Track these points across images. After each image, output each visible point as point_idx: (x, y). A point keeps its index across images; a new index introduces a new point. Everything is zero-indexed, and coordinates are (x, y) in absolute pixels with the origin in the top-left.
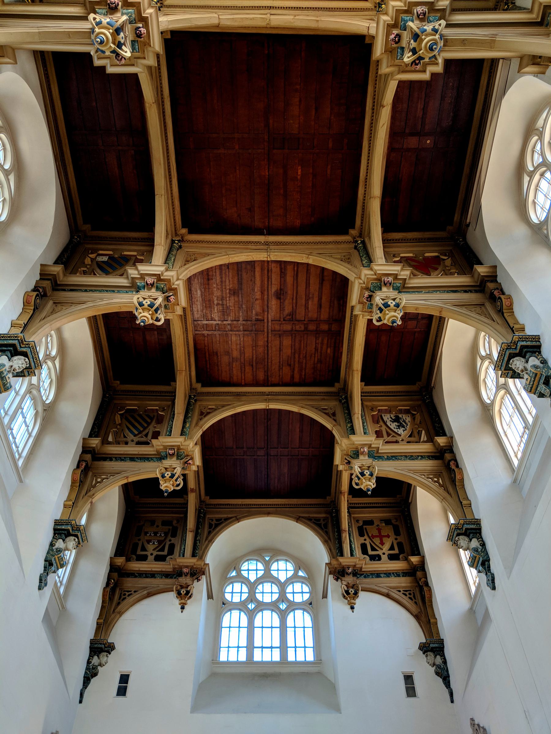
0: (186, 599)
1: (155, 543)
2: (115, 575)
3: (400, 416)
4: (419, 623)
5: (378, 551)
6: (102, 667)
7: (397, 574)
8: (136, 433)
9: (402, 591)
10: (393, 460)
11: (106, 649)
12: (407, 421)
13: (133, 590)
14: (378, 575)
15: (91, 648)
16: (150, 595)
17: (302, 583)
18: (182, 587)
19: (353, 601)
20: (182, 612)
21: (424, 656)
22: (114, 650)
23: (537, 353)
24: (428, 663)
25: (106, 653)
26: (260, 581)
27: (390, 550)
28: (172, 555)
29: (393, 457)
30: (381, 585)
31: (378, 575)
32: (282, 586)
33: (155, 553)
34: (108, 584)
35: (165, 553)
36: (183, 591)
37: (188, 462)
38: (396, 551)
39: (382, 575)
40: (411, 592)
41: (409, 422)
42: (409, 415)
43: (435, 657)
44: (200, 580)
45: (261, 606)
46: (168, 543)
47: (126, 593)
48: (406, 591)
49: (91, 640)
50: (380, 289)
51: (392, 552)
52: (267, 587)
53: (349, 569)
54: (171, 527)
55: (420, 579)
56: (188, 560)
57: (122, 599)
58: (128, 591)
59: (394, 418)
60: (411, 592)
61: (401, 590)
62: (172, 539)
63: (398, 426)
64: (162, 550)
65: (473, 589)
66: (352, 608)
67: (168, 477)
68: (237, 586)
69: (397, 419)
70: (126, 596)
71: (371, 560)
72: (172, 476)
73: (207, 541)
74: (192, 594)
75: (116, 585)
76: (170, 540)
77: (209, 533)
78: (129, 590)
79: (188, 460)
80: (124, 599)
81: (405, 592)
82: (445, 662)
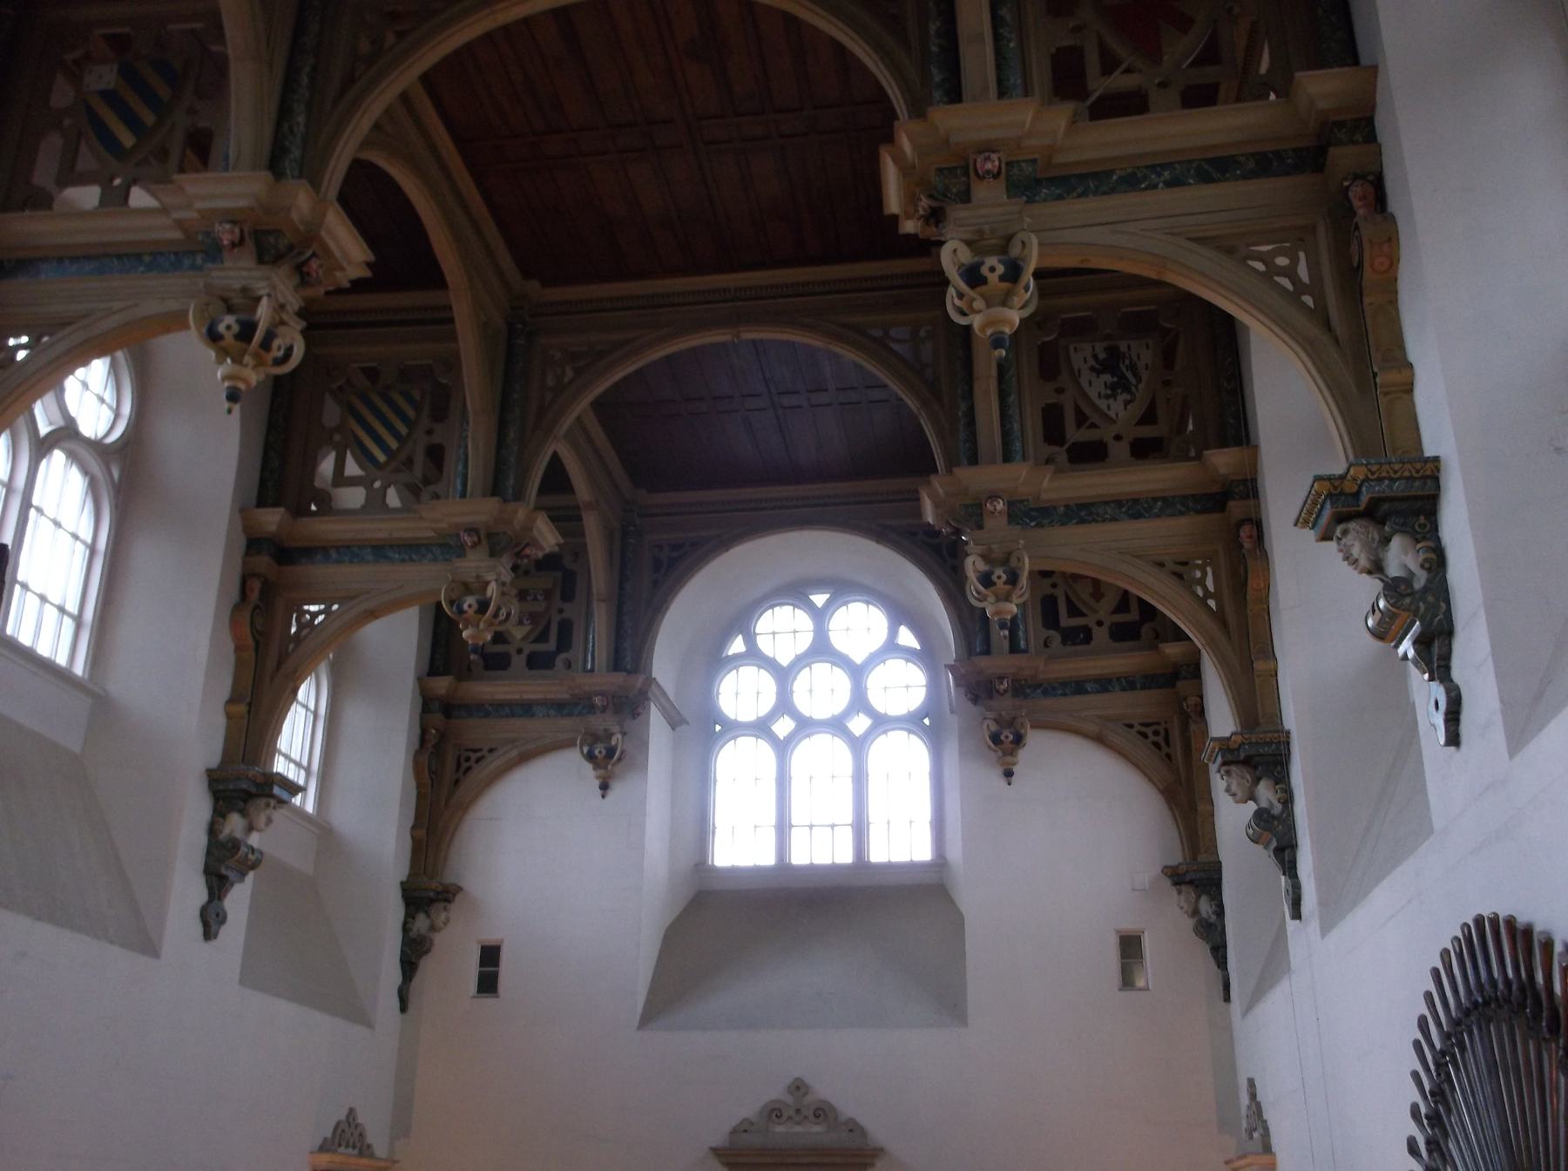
1: (526, 622)
2: (437, 718)
3: (1123, 346)
4: (1171, 809)
7: (1129, 683)
8: (382, 458)
9: (1136, 725)
10: (1082, 521)
11: (440, 897)
16: (525, 758)
19: (1009, 759)
20: (603, 797)
23: (1422, 519)
25: (442, 905)
26: (803, 661)
27: (1114, 612)
28: (567, 651)
29: (1083, 512)
32: (857, 673)
33: (529, 648)
34: (423, 740)
35: (551, 645)
36: (599, 750)
37: (523, 553)
38: (1134, 615)
40: (1161, 729)
41: (1147, 368)
44: (639, 714)
45: (806, 726)
46: (556, 619)
48: (1147, 725)
50: (965, 197)
51: (1119, 618)
53: (1002, 683)
54: (559, 574)
55: (1185, 699)
56: (605, 680)
57: (464, 765)
59: (1102, 356)
60: (1161, 729)
63: (1113, 387)
64: (542, 637)
66: (1009, 774)
67: (471, 611)
69: (1111, 363)
71: (1064, 642)
72: (483, 606)
75: (443, 736)
76: (561, 611)
77: (656, 583)
79: (520, 548)
80: (468, 769)
81: (1143, 729)
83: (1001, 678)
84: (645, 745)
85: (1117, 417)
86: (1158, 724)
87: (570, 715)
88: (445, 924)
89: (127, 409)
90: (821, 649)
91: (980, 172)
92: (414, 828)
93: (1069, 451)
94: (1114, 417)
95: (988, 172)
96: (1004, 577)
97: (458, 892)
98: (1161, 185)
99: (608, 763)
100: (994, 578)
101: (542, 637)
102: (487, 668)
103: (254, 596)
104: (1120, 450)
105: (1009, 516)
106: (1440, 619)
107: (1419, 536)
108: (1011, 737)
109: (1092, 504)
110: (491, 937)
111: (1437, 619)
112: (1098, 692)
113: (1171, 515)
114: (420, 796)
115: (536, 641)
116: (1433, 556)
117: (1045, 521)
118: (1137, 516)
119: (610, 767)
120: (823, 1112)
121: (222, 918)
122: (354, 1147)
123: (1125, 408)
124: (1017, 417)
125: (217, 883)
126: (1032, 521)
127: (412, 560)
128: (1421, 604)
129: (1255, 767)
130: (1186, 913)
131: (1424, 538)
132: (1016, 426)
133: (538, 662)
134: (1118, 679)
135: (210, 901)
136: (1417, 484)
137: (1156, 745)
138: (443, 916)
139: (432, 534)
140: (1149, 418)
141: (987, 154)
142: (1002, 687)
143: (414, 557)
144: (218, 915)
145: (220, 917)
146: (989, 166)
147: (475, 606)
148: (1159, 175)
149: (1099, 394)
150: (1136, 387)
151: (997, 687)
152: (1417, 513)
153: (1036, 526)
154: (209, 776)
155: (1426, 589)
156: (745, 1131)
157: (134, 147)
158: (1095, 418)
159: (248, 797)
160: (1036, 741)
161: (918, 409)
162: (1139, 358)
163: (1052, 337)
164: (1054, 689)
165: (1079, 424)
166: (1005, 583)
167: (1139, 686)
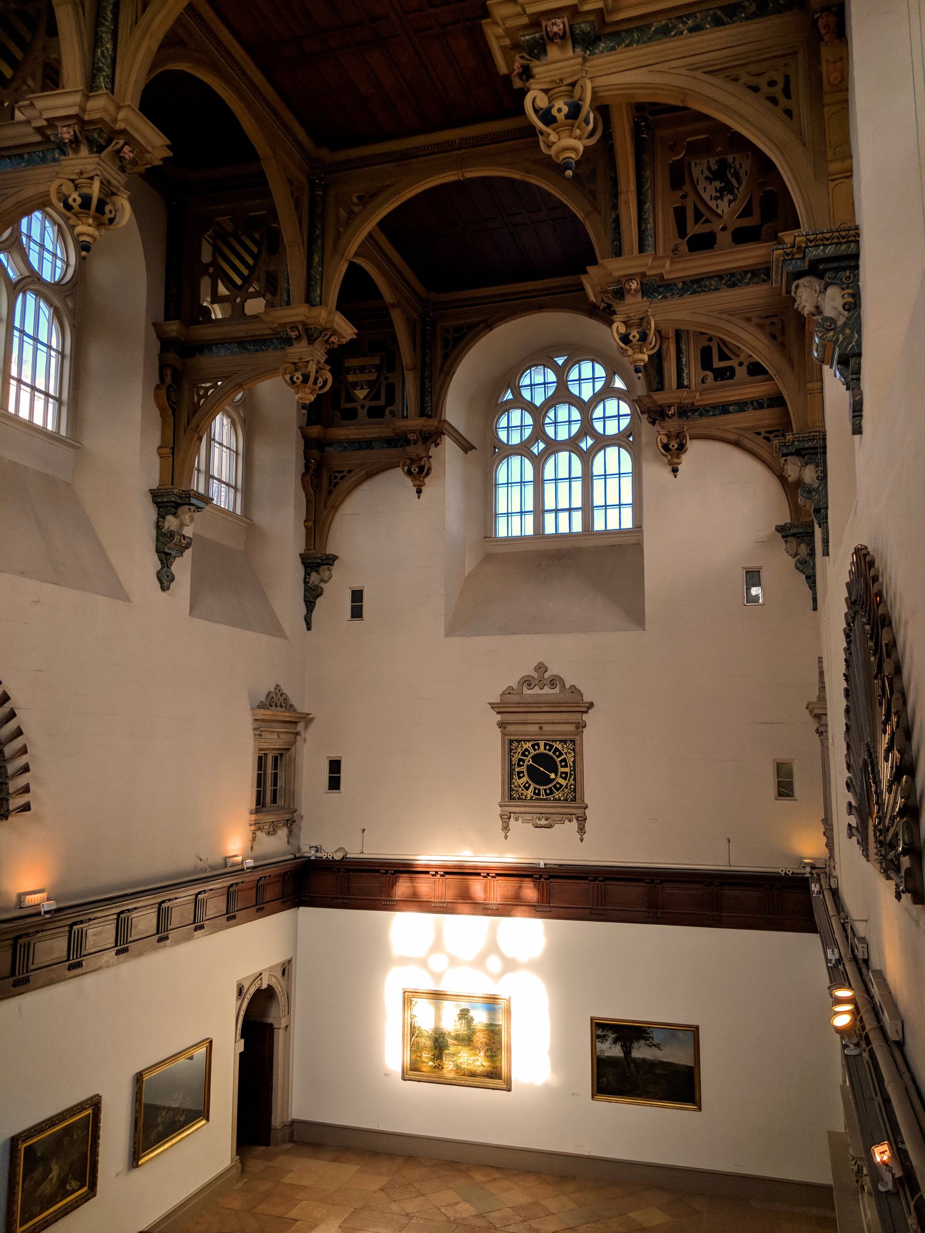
3: (730, 158)
4: (784, 488)
5: (731, 359)
6: (326, 583)
10: (694, 292)
12: (742, 172)
13: (346, 470)
14: (724, 409)
16: (369, 475)
17: (619, 399)
18: (413, 461)
19: (676, 461)
20: (419, 498)
21: (782, 541)
24: (787, 552)
30: (727, 427)
31: (724, 409)
33: (368, 404)
34: (307, 467)
35: (382, 402)
36: (415, 469)
39: (731, 409)
41: (746, 174)
42: (750, 154)
43: (799, 544)
44: (438, 444)
47: (337, 474)
52: (563, 412)
53: (670, 410)
58: (340, 472)
59: (714, 167)
61: (762, 431)
62: (389, 375)
64: (376, 397)
66: (675, 471)
68: (516, 416)
69: (719, 174)
70: (338, 479)
71: (716, 379)
73: (443, 375)
75: (320, 466)
76: (386, 378)
77: (446, 357)
78: (341, 470)
80: (337, 483)
81: (767, 435)
83: (670, 406)
84: (444, 462)
85: (723, 213)
87: (396, 447)
89: (73, 261)
90: (562, 395)
91: (551, 35)
92: (305, 521)
93: (689, 243)
94: (721, 214)
95: (556, 34)
96: (638, 336)
97: (336, 559)
98: (686, 32)
99: (420, 477)
100: (631, 337)
101: (376, 397)
102: (343, 419)
103: (168, 380)
104: (724, 238)
105: (643, 293)
106: (853, 345)
107: (845, 286)
108: (676, 446)
109: (702, 279)
110: (357, 586)
111: (850, 346)
112: (738, 412)
113: (758, 283)
114: (308, 502)
115: (371, 400)
116: (851, 300)
117: (668, 295)
118: (733, 285)
119: (421, 479)
120: (555, 681)
121: (172, 579)
122: (281, 707)
123: (729, 207)
124: (651, 220)
125: (165, 557)
126: (659, 295)
127: (263, 350)
128: (841, 336)
129: (803, 457)
131: (848, 287)
132: (650, 226)
133: (376, 413)
134: (752, 402)
135: (162, 568)
136: (844, 247)
138: (327, 573)
139: (270, 332)
140: (746, 212)
141: (553, 21)
142: (670, 412)
143: (263, 347)
144: (168, 576)
145: (170, 577)
146: (555, 29)
147: (301, 378)
148: (685, 23)
149: (711, 196)
150: (738, 189)
151: (667, 412)
152: (844, 269)
153: (663, 297)
154: (151, 494)
155: (845, 325)
156: (510, 693)
157: (13, 77)
158: (708, 215)
159: (177, 505)
160: (696, 450)
161: (584, 219)
162: (741, 167)
163: (682, 155)
164: (707, 411)
165: (696, 222)
166: (638, 341)
167: (765, 405)
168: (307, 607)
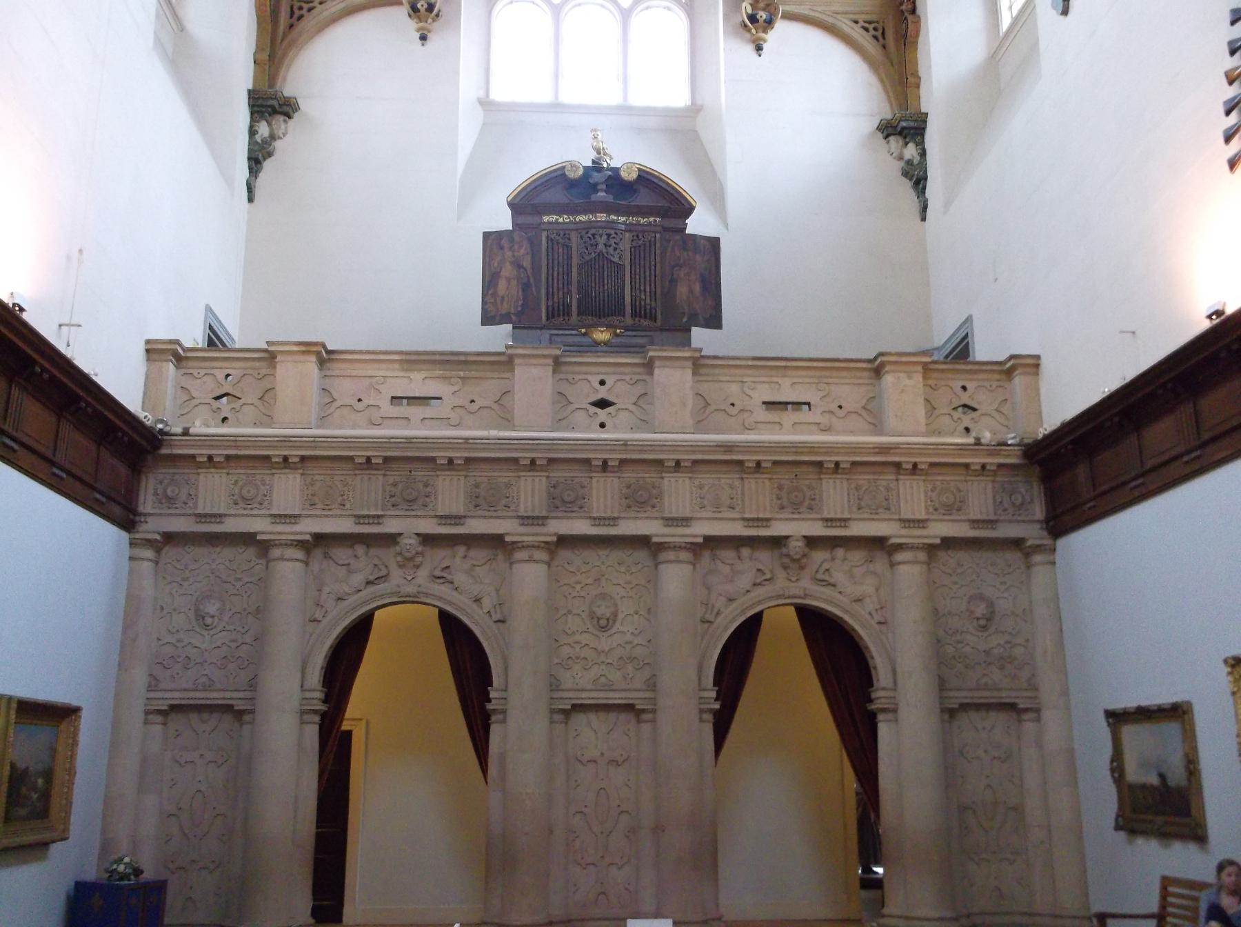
0: (430, 20)
15: (251, 106)
22: (297, 111)
48: (870, 23)
49: (249, 91)
65: (1006, 22)
74: (439, 11)
81: (866, 25)
82: (923, 154)
86: (877, 22)
88: (284, 135)
92: (255, 54)
130: (895, 158)
137: (875, 37)
168: (250, 169)
